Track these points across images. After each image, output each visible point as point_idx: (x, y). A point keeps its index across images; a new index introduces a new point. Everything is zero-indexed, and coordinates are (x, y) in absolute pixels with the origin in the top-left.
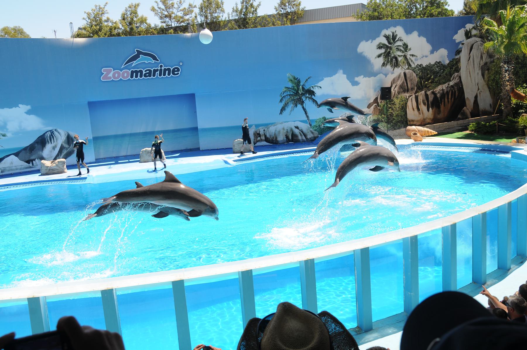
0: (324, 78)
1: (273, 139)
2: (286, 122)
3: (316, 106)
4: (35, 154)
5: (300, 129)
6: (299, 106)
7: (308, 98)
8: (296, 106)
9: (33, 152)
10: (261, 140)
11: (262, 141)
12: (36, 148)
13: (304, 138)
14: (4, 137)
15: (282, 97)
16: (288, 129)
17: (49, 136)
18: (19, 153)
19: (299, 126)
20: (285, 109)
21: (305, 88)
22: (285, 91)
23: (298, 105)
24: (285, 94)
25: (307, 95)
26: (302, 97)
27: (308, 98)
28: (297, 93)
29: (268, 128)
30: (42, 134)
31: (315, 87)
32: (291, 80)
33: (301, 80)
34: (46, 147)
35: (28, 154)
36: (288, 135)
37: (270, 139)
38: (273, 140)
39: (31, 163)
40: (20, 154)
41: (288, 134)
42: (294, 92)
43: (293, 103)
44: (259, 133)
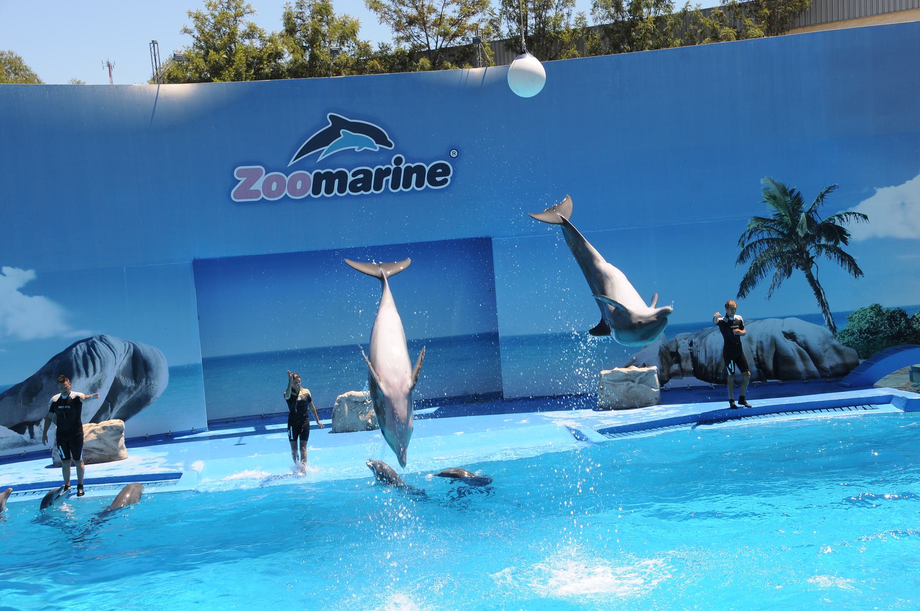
0: (875, 188)
1: (717, 369)
2: (755, 320)
3: (850, 272)
4: (39, 406)
5: (800, 339)
6: (798, 274)
7: (824, 250)
8: (789, 273)
9: (34, 399)
10: (682, 373)
11: (683, 376)
13: (813, 368)
15: (745, 245)
16: (763, 339)
17: (81, 354)
19: (798, 332)
20: (753, 283)
21: (816, 218)
22: (756, 229)
23: (794, 270)
24: (754, 239)
25: (823, 241)
26: (805, 246)
27: (824, 250)
28: (790, 235)
29: (701, 338)
31: (848, 216)
32: (774, 198)
33: (804, 195)
36: (763, 359)
37: (709, 369)
38: (717, 373)
39: (27, 431)
41: (762, 355)
42: (781, 233)
43: (778, 265)
44: (677, 351)
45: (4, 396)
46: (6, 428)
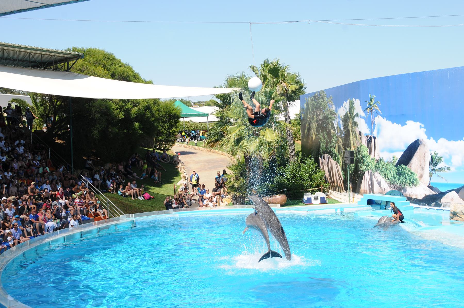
14: (448, 171)
18: (460, 190)
40: (460, 191)
45: (462, 188)
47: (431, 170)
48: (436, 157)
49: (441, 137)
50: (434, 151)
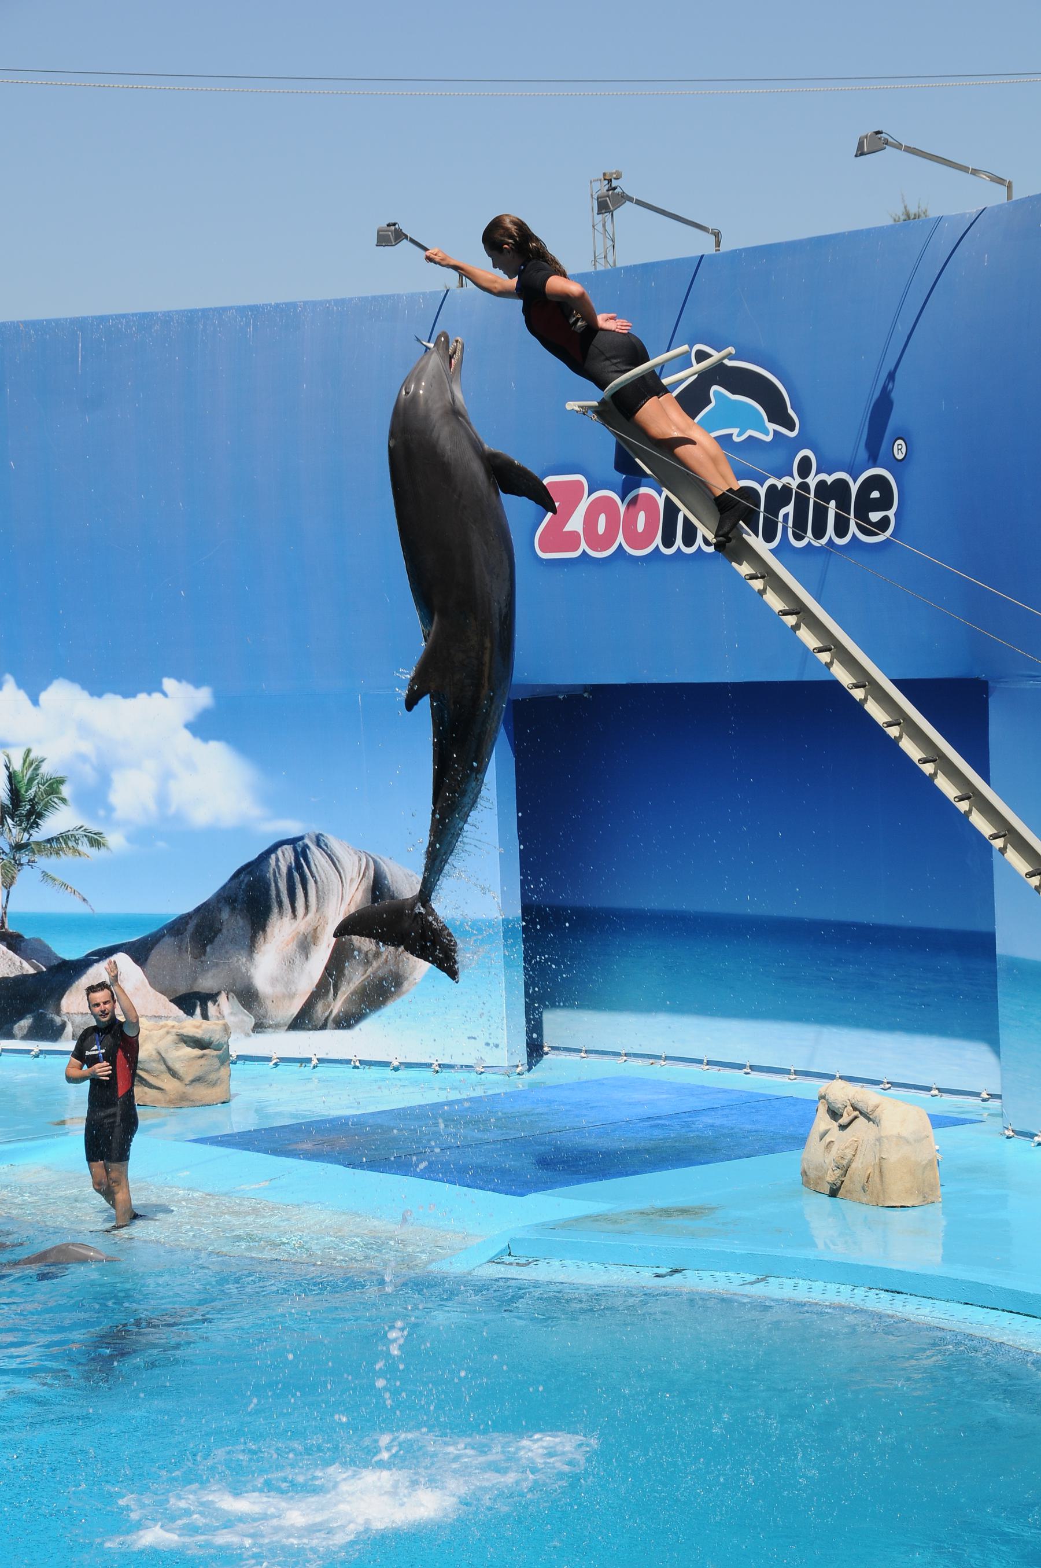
4: (217, 965)
9: (208, 949)
12: (224, 931)
17: (284, 870)
30: (257, 856)
34: (269, 930)
35: (188, 958)
39: (198, 1011)
45: (163, 936)
46: (164, 999)
47: (7, 851)
48: (31, 780)
49: (57, 678)
50: (23, 750)
